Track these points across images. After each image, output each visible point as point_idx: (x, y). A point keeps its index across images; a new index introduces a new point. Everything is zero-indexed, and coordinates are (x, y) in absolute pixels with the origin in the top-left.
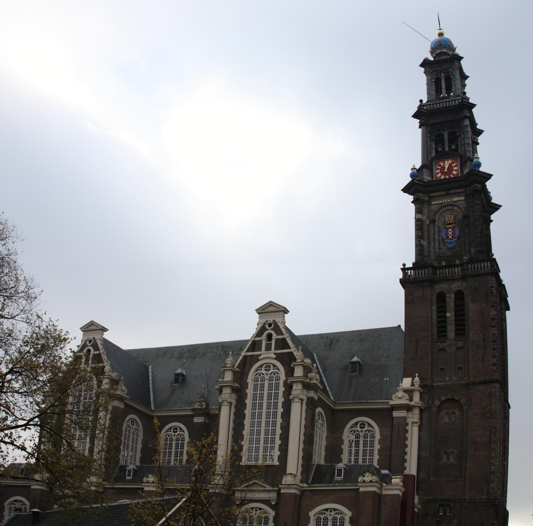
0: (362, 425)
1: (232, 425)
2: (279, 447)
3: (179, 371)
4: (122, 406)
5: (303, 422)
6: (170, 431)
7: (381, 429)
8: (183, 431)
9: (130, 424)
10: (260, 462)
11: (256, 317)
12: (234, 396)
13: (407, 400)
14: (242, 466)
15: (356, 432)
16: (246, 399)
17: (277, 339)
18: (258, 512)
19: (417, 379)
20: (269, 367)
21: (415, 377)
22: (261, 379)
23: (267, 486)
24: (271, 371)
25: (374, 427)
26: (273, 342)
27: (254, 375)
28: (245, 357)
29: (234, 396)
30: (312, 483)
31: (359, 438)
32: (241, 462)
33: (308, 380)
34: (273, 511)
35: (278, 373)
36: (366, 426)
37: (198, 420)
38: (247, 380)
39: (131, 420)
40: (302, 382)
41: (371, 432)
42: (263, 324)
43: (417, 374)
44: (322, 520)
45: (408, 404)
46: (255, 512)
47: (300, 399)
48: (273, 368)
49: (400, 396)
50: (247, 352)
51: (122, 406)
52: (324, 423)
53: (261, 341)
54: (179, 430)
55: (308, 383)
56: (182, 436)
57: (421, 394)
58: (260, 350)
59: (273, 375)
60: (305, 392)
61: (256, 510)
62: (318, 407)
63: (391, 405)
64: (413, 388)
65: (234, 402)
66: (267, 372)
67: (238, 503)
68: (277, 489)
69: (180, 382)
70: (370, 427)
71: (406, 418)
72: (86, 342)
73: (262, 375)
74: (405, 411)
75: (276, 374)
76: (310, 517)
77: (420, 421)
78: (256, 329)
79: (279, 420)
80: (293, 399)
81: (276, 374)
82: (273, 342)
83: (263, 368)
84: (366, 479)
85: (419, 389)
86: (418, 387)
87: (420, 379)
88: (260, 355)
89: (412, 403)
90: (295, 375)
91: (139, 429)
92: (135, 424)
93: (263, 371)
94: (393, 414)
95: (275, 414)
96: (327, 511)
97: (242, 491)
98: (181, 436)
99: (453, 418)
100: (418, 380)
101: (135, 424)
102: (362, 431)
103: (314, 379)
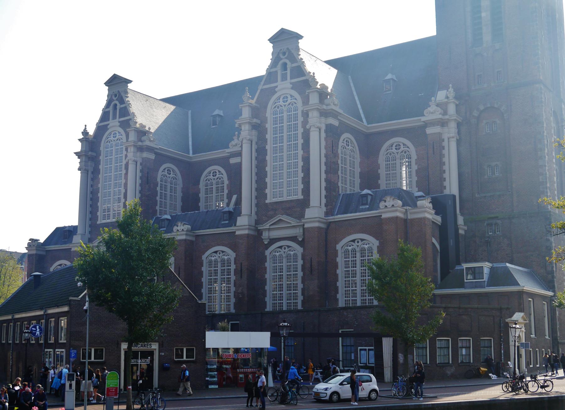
0: (398, 147)
1: (254, 162)
2: (302, 180)
3: (217, 112)
4: (152, 157)
5: (323, 151)
6: (210, 176)
7: (417, 148)
8: (222, 174)
9: (166, 173)
10: (285, 198)
11: (269, 48)
12: (254, 132)
13: (440, 114)
14: (267, 203)
15: (392, 155)
17: (292, 67)
18: (287, 250)
19: (451, 90)
20: (287, 97)
21: (449, 88)
22: (294, 108)
23: (293, 223)
24: (289, 101)
25: (410, 147)
26: (288, 72)
27: (272, 108)
28: (262, 90)
29: (254, 132)
30: (337, 215)
31: (395, 161)
32: (267, 199)
33: (325, 107)
35: (295, 103)
36: (402, 146)
37: (233, 161)
38: (265, 115)
39: (166, 171)
40: (318, 109)
41: (407, 153)
42: (277, 54)
43: (451, 85)
44: (350, 253)
45: (441, 118)
46: (284, 250)
47: (317, 127)
49: (432, 111)
50: (264, 85)
51: (152, 157)
52: (356, 149)
53: (276, 72)
54: (218, 173)
55: (324, 109)
56: (221, 179)
57: (457, 105)
58: (277, 81)
59: (291, 105)
60: (323, 119)
61: (285, 249)
62: (343, 133)
63: (424, 122)
64: (446, 100)
65: (255, 140)
66: (285, 104)
67: (266, 243)
68: (303, 224)
69: (217, 124)
70: (406, 147)
71: (441, 134)
72: (111, 97)
73: (280, 108)
74: (439, 126)
75: (294, 105)
76: (337, 251)
77: (458, 135)
78: (271, 59)
79: (300, 153)
80: (310, 128)
81: (294, 105)
82: (288, 72)
83: (281, 100)
84: (386, 204)
85: (453, 100)
86: (452, 98)
87: (455, 90)
88: (277, 87)
89: (447, 117)
90: (311, 102)
91: (177, 178)
92: (172, 172)
93: (281, 103)
94: (426, 131)
95: (296, 145)
96: (354, 242)
97: (269, 230)
98: (220, 179)
99: (495, 128)
100: (452, 91)
101: (172, 172)
102: (398, 153)
103: (332, 104)
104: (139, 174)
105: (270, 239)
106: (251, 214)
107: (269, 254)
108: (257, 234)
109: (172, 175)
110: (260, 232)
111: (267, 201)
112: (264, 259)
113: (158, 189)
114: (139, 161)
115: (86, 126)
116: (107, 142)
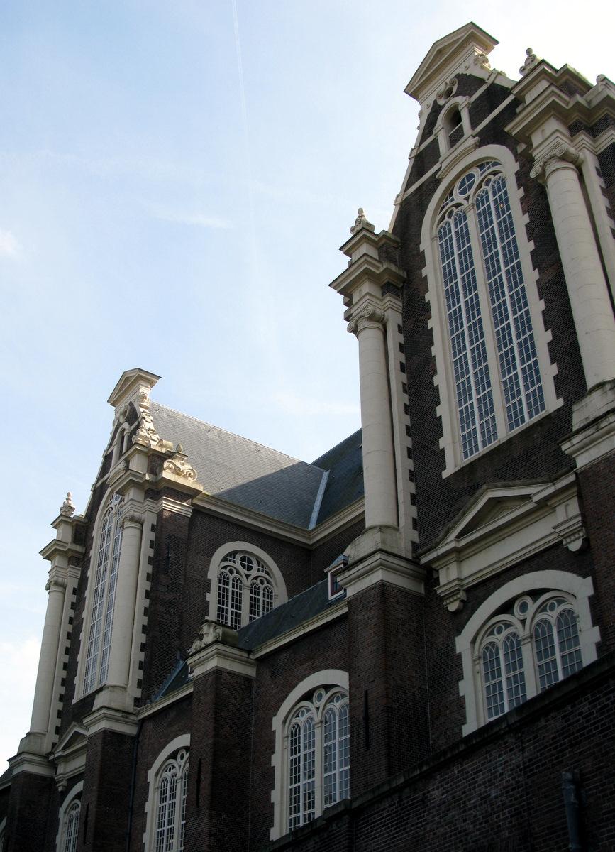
2: (551, 351)
9: (238, 565)
10: (503, 433)
12: (388, 298)
16: (427, 290)
29: (388, 299)
34: (585, 577)
35: (495, 173)
39: (238, 557)
48: (480, 173)
65: (394, 319)
67: (453, 607)
68: (572, 478)
78: (418, 128)
92: (255, 565)
101: (255, 565)
104: (147, 552)
105: (468, 591)
106: (398, 525)
107: (468, 645)
108: (423, 591)
109: (254, 573)
110: (428, 575)
111: (445, 474)
112: (450, 668)
113: (212, 597)
114: (150, 519)
115: (69, 495)
116: (105, 515)
